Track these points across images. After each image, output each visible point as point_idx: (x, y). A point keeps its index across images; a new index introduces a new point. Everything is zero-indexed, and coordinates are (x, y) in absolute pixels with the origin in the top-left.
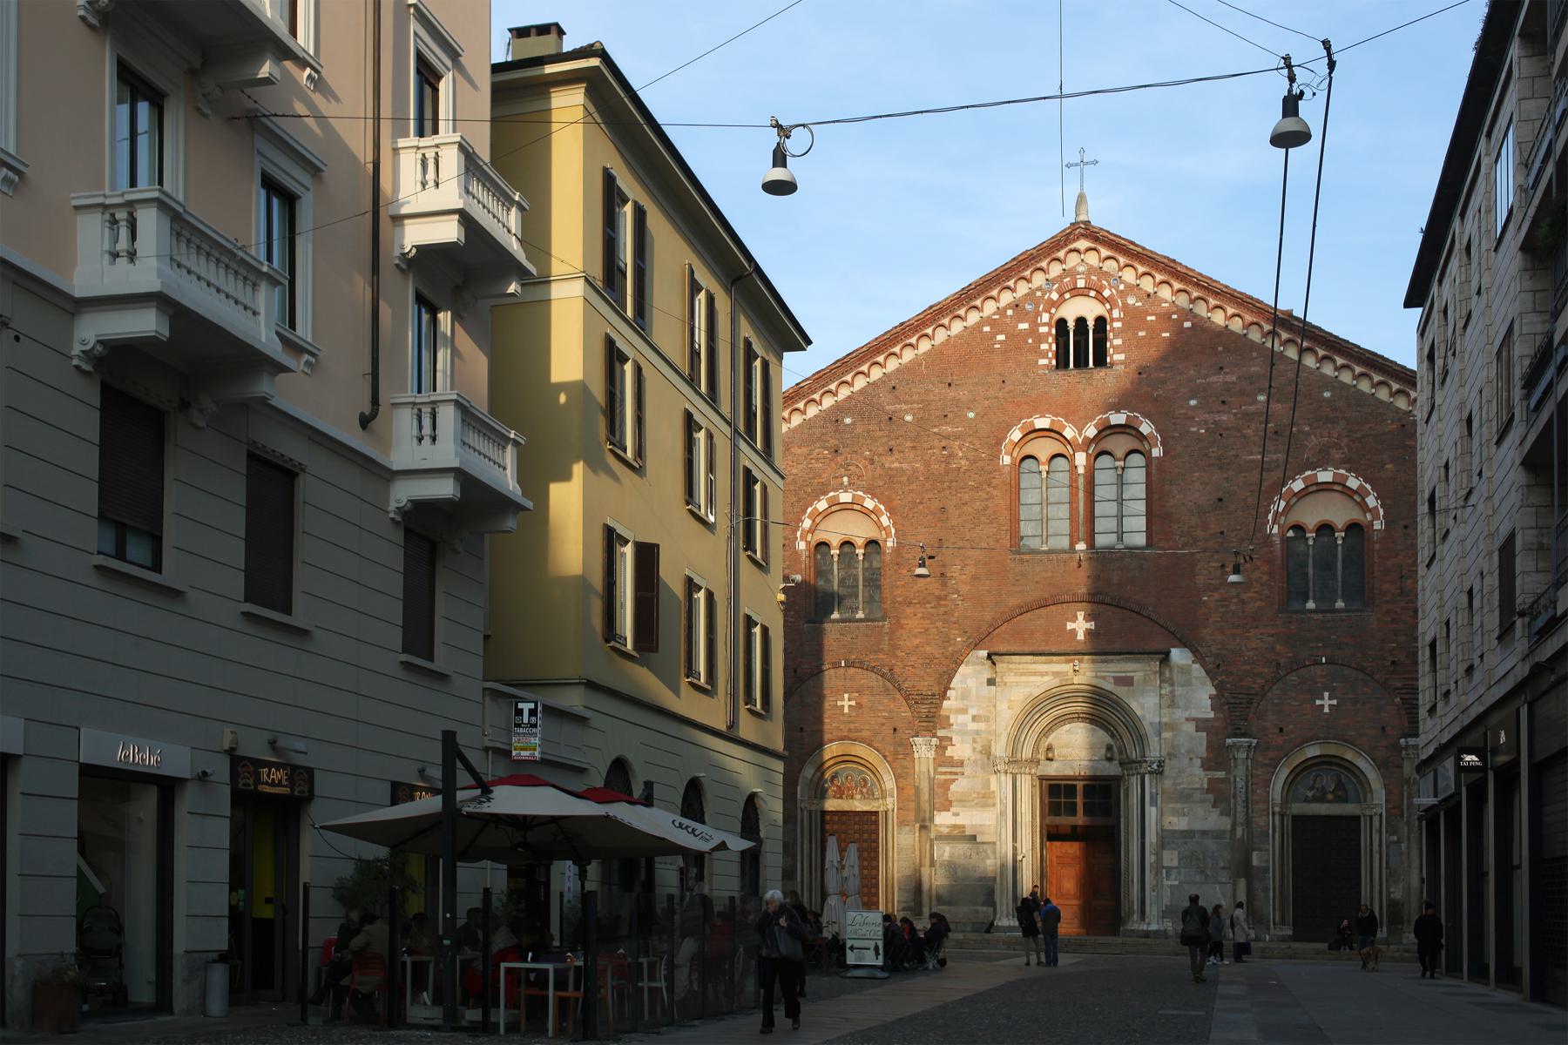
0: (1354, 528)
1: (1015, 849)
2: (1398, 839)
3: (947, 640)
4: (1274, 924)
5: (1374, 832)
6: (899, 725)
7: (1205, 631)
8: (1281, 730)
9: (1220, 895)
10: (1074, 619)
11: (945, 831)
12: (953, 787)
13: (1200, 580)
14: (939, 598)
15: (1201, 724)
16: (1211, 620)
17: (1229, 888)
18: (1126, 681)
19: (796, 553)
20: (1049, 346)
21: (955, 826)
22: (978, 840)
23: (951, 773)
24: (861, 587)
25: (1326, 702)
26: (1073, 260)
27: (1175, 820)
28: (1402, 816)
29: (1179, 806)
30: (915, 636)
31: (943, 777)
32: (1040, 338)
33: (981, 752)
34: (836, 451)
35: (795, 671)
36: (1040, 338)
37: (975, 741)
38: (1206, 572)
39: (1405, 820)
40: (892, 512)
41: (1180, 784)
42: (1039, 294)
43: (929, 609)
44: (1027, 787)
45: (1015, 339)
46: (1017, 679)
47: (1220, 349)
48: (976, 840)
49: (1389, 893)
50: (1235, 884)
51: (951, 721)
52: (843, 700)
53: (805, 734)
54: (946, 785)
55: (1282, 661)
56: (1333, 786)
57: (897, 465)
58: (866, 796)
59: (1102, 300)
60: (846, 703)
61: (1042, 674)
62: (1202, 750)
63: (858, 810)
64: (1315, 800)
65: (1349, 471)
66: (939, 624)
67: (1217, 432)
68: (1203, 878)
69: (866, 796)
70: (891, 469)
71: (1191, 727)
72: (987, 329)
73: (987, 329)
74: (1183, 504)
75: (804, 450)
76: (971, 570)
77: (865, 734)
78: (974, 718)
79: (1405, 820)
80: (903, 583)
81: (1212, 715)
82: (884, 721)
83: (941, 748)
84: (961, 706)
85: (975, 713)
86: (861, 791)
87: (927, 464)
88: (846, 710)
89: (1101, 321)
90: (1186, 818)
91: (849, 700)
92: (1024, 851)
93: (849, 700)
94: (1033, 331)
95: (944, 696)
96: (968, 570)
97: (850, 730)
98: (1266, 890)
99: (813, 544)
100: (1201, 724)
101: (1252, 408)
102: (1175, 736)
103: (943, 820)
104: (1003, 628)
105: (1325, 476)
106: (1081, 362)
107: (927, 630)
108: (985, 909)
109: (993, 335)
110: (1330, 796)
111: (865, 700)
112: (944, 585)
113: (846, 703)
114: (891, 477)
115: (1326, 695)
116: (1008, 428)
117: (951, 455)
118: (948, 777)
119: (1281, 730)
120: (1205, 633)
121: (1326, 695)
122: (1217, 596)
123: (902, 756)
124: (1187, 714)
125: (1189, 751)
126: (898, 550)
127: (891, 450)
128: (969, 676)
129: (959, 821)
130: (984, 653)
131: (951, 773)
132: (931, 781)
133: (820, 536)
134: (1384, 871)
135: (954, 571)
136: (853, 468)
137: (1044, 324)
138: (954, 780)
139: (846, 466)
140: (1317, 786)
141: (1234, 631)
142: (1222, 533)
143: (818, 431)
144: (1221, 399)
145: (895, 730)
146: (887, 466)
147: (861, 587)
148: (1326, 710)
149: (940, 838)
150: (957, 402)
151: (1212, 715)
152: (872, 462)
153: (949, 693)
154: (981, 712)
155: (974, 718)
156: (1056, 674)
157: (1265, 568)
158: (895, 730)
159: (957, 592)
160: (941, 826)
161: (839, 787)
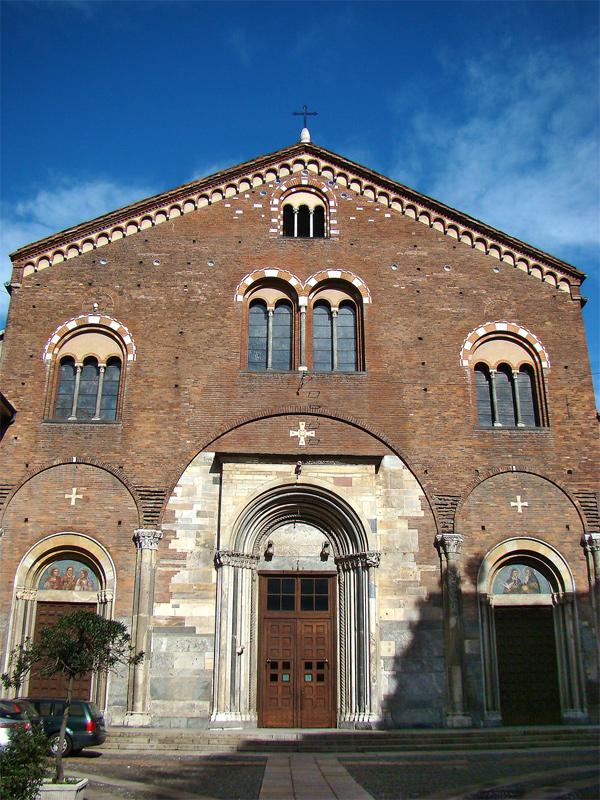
0: (525, 368)
1: (234, 641)
2: (590, 624)
3: (177, 441)
4: (488, 710)
5: (567, 617)
6: (125, 519)
7: (412, 441)
8: (483, 528)
9: (435, 684)
10: (297, 428)
11: (164, 622)
12: (175, 580)
13: (407, 400)
14: (172, 406)
15: (413, 523)
16: (418, 433)
17: (445, 676)
18: (347, 482)
19: (42, 363)
20: (278, 221)
21: (174, 619)
22: (197, 632)
23: (173, 565)
24: (100, 395)
25: (519, 504)
26: (298, 168)
27: (390, 611)
28: (591, 604)
29: (395, 598)
30: (147, 438)
31: (163, 569)
32: (272, 215)
33: (204, 546)
34: (90, 284)
35: (27, 466)
36: (272, 215)
37: (198, 535)
38: (412, 394)
39: (594, 606)
40: (134, 333)
41: (396, 577)
42: (271, 186)
43: (162, 414)
44: (246, 578)
45: (251, 217)
46: (242, 477)
47: (414, 233)
48: (195, 632)
49: (586, 675)
50: (450, 672)
51: (177, 516)
52: (71, 493)
53: (28, 524)
54: (168, 577)
55: (480, 468)
56: (527, 578)
57: (143, 297)
58: (86, 587)
59: (319, 194)
60: (73, 497)
61: (267, 473)
62: (414, 546)
63: (76, 601)
64: (513, 591)
65: (519, 324)
66: (170, 428)
67: (414, 289)
68: (419, 667)
69: (86, 587)
70: (136, 299)
71: (403, 525)
72: (228, 205)
73: (228, 205)
74: (391, 340)
75: (62, 282)
76: (203, 383)
77: (89, 526)
78: (199, 514)
79: (594, 606)
80: (139, 391)
81: (422, 514)
82: (110, 514)
83: (163, 540)
84: (186, 502)
85: (200, 509)
86: (81, 583)
87: (170, 298)
88: (73, 503)
89: (319, 210)
90: (402, 610)
91: (77, 494)
92: (243, 644)
93: (77, 494)
94: (266, 209)
95: (171, 492)
96: (200, 383)
97: (75, 522)
98: (478, 676)
99: (59, 357)
100: (413, 523)
101: (441, 275)
102: (389, 533)
103: (163, 611)
104: (230, 434)
105: (501, 327)
106: (304, 232)
107: (158, 432)
108: (201, 703)
109: (232, 211)
110: (525, 588)
111: (92, 494)
112: (178, 394)
113: (73, 497)
114: (136, 306)
115: (519, 498)
116: (242, 275)
117: (193, 292)
118: (170, 569)
119: (483, 528)
120: (413, 443)
121: (519, 498)
122: (421, 413)
123: (124, 548)
124: (400, 513)
125: (402, 547)
126: (137, 364)
127: (139, 286)
128: (196, 476)
129: (179, 613)
130: (213, 455)
131: (173, 565)
132: (153, 571)
133: (67, 350)
134: (580, 654)
135: (187, 383)
136: (103, 298)
137: (275, 206)
138: (176, 573)
139: (98, 295)
140: (514, 579)
141: (438, 443)
142: (423, 364)
143: (75, 268)
144: (417, 266)
145: (120, 523)
146: (134, 297)
147: (100, 395)
148: (520, 511)
149: (159, 630)
150: (199, 254)
151: (422, 514)
152: (121, 293)
153: (176, 490)
154: (206, 509)
155: (199, 514)
156: (279, 474)
157: (460, 392)
158: (120, 523)
159: (189, 400)
160: (160, 618)
161: (59, 578)
